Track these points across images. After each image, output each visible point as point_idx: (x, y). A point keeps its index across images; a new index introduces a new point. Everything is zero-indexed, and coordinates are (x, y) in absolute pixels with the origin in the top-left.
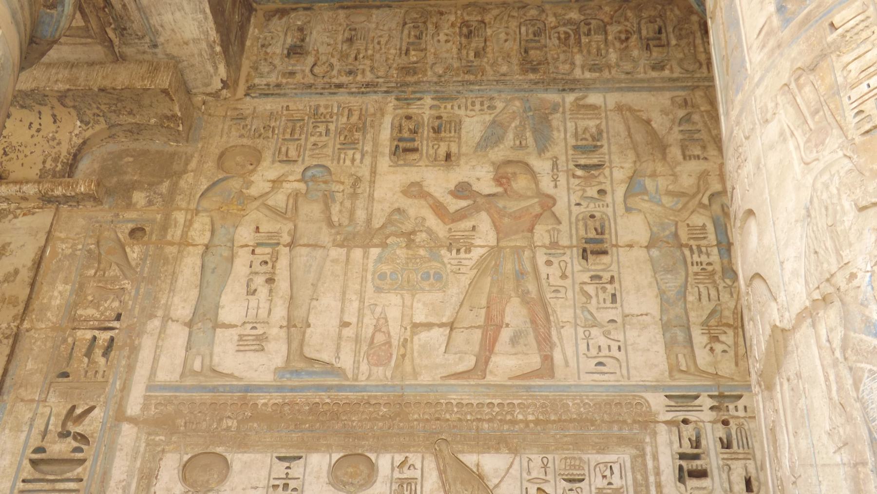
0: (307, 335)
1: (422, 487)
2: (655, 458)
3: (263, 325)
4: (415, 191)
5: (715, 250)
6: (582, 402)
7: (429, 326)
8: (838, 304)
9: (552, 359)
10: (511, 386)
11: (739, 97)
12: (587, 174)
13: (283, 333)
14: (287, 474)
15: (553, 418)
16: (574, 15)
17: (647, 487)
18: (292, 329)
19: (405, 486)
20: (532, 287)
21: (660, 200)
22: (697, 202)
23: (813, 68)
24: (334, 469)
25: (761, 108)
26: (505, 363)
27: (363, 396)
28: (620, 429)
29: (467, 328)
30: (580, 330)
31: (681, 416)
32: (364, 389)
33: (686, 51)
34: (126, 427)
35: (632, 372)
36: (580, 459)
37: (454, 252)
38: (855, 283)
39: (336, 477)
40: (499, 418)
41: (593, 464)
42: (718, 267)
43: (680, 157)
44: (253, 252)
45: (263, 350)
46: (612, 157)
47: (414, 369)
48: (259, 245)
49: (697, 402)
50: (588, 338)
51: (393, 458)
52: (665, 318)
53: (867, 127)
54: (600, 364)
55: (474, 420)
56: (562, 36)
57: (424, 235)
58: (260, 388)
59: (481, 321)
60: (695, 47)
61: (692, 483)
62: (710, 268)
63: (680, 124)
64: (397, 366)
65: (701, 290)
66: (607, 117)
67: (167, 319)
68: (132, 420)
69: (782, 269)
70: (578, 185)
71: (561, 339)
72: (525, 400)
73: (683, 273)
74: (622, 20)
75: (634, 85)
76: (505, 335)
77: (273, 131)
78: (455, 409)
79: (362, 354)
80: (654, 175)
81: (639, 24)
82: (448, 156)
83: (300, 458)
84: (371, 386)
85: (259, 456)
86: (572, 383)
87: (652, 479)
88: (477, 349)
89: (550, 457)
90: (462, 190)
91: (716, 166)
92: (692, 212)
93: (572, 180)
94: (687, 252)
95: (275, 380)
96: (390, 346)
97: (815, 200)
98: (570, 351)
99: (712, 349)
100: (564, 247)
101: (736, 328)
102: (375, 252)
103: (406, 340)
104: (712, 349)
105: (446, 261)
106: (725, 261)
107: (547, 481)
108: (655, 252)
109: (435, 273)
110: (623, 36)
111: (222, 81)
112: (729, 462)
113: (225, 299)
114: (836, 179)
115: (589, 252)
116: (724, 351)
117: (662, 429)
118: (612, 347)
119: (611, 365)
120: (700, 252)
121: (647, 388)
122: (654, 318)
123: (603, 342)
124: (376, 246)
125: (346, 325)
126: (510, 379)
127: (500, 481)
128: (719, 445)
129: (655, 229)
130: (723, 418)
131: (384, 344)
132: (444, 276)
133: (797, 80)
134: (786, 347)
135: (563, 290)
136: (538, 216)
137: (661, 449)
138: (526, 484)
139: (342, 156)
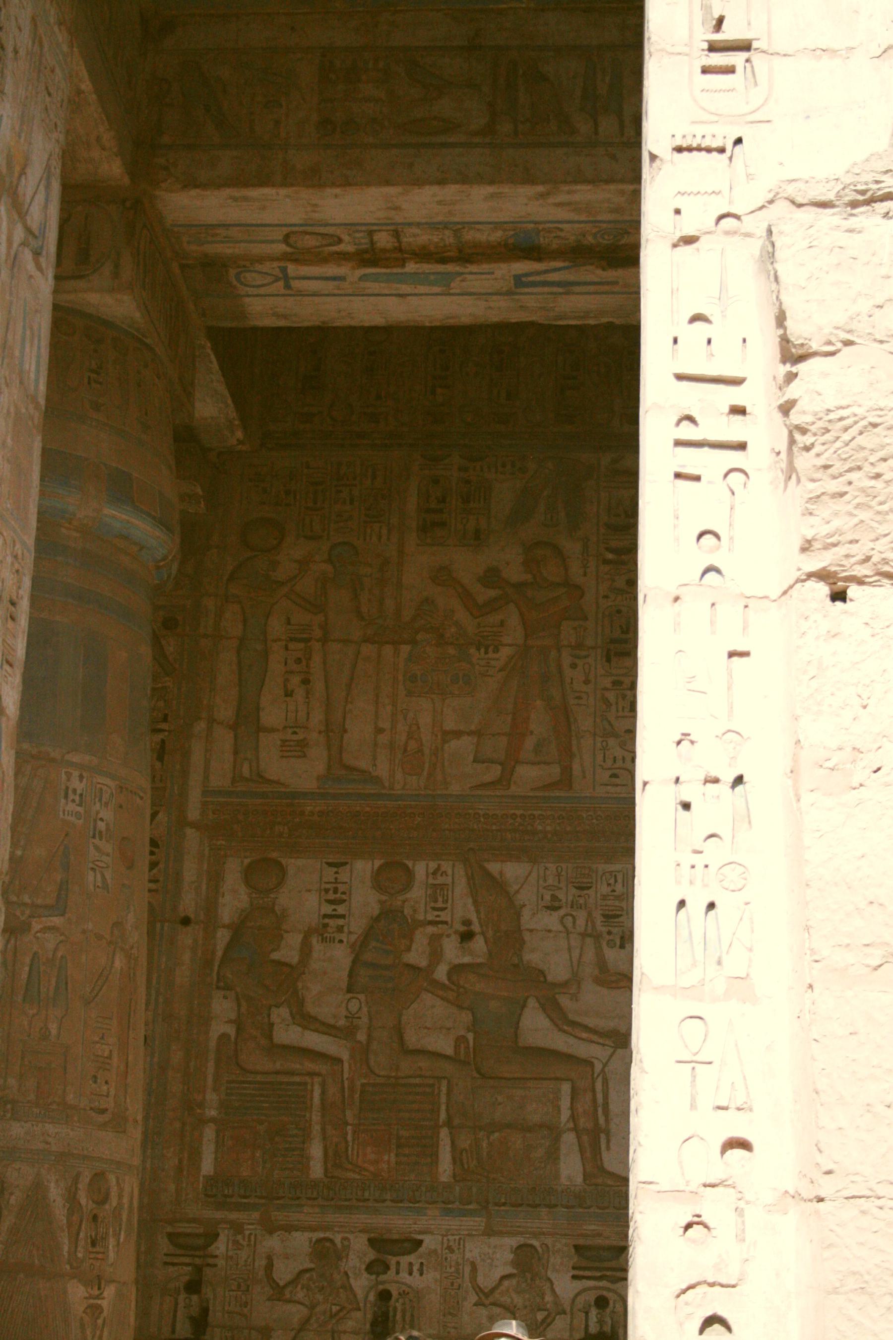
3: (302, 730)
4: (442, 576)
7: (458, 734)
9: (571, 768)
10: (532, 797)
14: (336, 879)
15: (569, 829)
18: (331, 734)
24: (377, 875)
26: (528, 775)
34: (189, 831)
36: (590, 868)
37: (483, 650)
41: (600, 873)
44: (287, 648)
45: (305, 756)
48: (292, 640)
51: (427, 865)
58: (305, 795)
67: (211, 721)
68: (194, 825)
76: (529, 743)
77: (295, 498)
78: (482, 820)
79: (397, 762)
82: (477, 535)
83: (346, 863)
86: (588, 795)
90: (491, 577)
95: (319, 788)
96: (423, 755)
102: (405, 649)
107: (561, 889)
111: (238, 440)
124: (405, 643)
139: (369, 531)
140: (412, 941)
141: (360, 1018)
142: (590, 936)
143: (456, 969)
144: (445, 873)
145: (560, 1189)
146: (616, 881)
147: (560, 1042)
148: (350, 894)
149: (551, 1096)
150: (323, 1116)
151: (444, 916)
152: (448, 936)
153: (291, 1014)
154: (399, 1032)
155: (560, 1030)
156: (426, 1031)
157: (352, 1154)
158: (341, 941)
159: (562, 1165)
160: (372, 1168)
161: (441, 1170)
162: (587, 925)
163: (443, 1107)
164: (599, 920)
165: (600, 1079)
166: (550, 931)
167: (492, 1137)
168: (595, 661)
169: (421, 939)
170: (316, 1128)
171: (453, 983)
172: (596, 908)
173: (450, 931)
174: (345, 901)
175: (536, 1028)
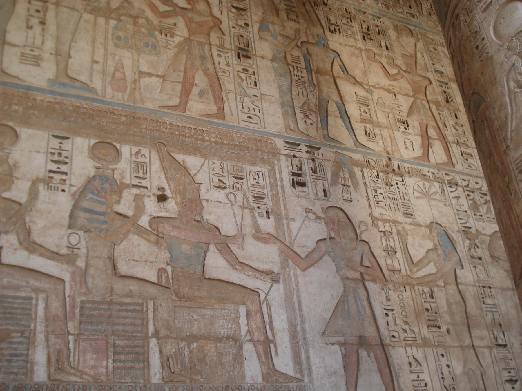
0: (69, 63)
1: (150, 169)
2: (280, 172)
5: (305, 71)
6: (241, 136)
7: (150, 75)
10: (201, 120)
12: (237, 13)
13: (53, 58)
14: (60, 147)
15: (225, 142)
17: (277, 187)
18: (59, 57)
19: (140, 166)
20: (210, 67)
21: (277, 37)
22: (295, 44)
26: (197, 107)
27: (109, 108)
28: (262, 155)
29: (172, 82)
30: (238, 97)
31: (292, 153)
32: (109, 103)
35: (267, 125)
37: (163, 35)
39: (94, 154)
40: (195, 136)
41: (248, 171)
42: (307, 80)
43: (286, 18)
46: (251, 7)
47: (142, 98)
49: (299, 147)
50: (242, 102)
51: (131, 148)
52: (282, 100)
54: (249, 117)
55: (180, 135)
57: (144, 20)
59: (181, 79)
61: (299, 188)
62: (303, 80)
64: (130, 95)
65: (299, 90)
70: (233, 17)
71: (228, 99)
72: (210, 129)
76: (195, 90)
78: (169, 127)
79: (107, 82)
80: (273, 23)
83: (68, 138)
84: (115, 103)
85: (39, 132)
87: (279, 183)
88: (179, 94)
89: (225, 163)
93: (230, 13)
98: (233, 107)
99: (305, 121)
100: (227, 49)
103: (135, 80)
104: (305, 121)
105: (159, 39)
108: (275, 65)
109: (152, 45)
112: (316, 181)
113: (11, 27)
115: (241, 55)
116: (311, 124)
117: (283, 158)
118: (256, 110)
119: (255, 119)
120: (298, 70)
121: (275, 135)
122: (276, 99)
123: (251, 106)
125: (96, 62)
126: (200, 115)
127: (197, 172)
128: (311, 170)
130: (313, 158)
131: (122, 79)
132: (158, 48)
135: (228, 73)
136: (212, 28)
137: (283, 168)
138: (212, 176)
140: (120, 197)
141: (79, 248)
142: (247, 208)
143: (155, 220)
144: (143, 155)
145: (246, 387)
146: (259, 177)
147: (235, 277)
148: (71, 159)
149: (232, 315)
150: (47, 326)
151: (144, 183)
152: (149, 197)
153: (19, 239)
154: (112, 261)
155: (234, 268)
156: (134, 262)
157: (74, 361)
158: (63, 191)
159: (246, 368)
160: (92, 373)
161: (152, 373)
162: (244, 201)
163: (151, 323)
164: (251, 199)
165: (265, 304)
166: (220, 202)
167: (192, 347)
168: (232, 56)
169: (128, 195)
170: (40, 337)
171: (154, 230)
172: (249, 192)
173: (149, 194)
174: (67, 163)
175: (216, 265)
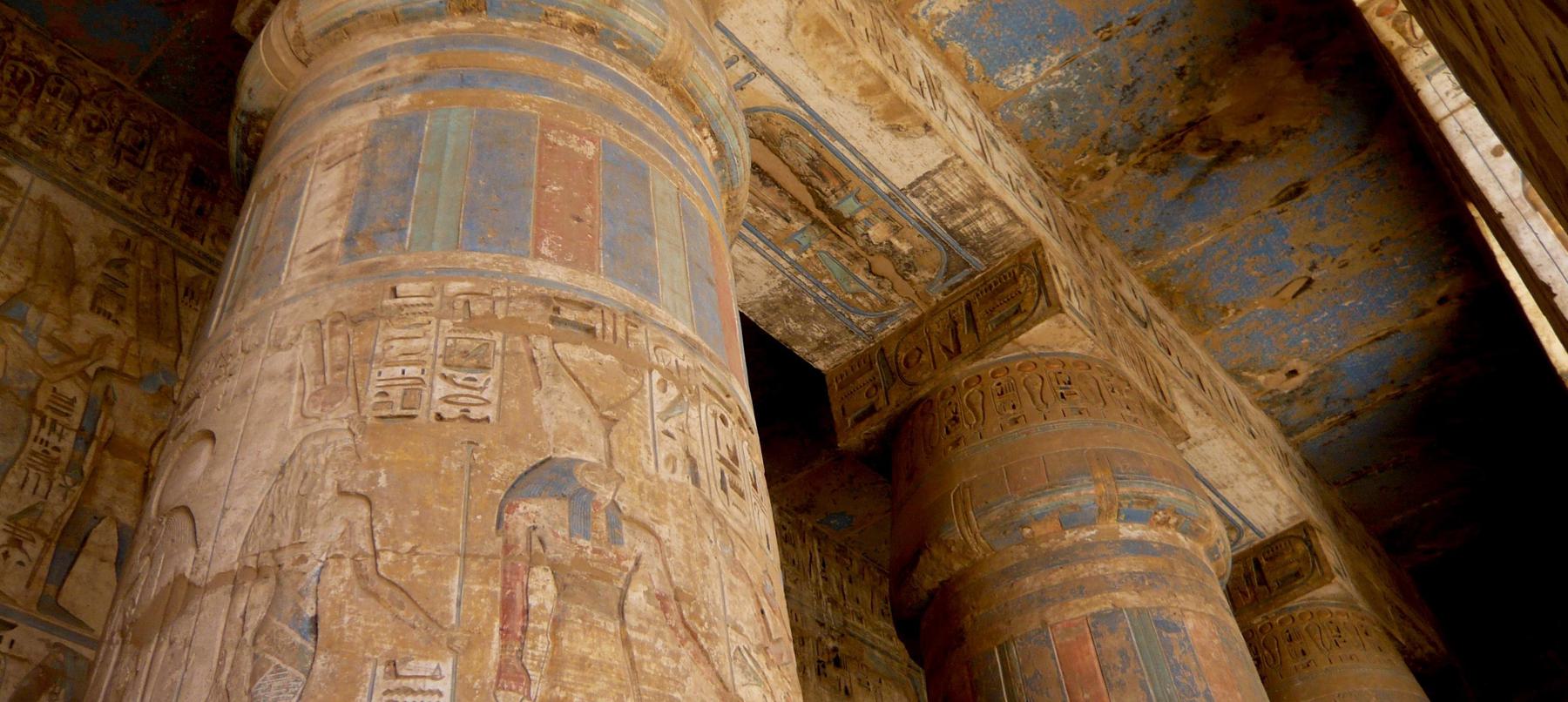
5: (72, 436)
8: (272, 581)
11: (257, 302)
16: (49, 61)
23: (356, 322)
25: (279, 330)
33: (159, 187)
38: (303, 567)
42: (65, 458)
43: (87, 303)
53: (384, 413)
56: (19, 75)
60: (171, 188)
62: (55, 454)
63: (107, 266)
65: (31, 476)
66: (22, 204)
69: (223, 516)
73: (18, 445)
74: (104, 105)
75: (76, 188)
80: (43, 308)
81: (121, 122)
91: (125, 338)
92: (68, 377)
94: (36, 422)
97: (297, 459)
101: (50, 540)
106: (78, 454)
110: (95, 124)
114: (330, 450)
120: (53, 429)
129: (10, 374)
133: (334, 323)
134: (185, 604)
